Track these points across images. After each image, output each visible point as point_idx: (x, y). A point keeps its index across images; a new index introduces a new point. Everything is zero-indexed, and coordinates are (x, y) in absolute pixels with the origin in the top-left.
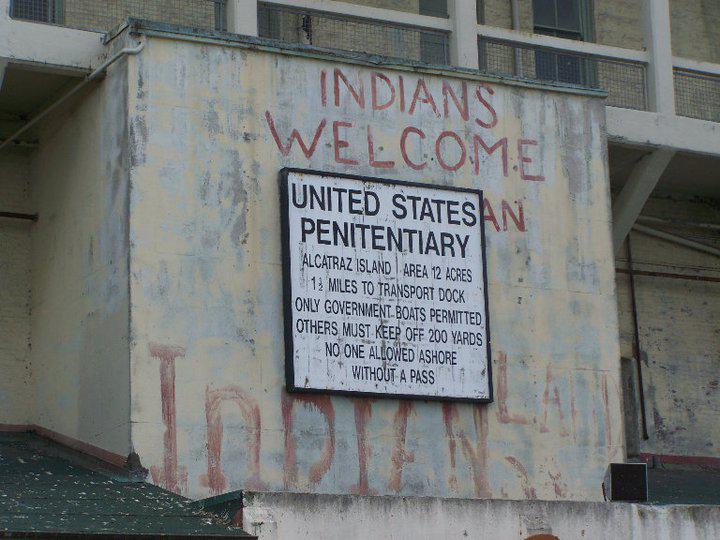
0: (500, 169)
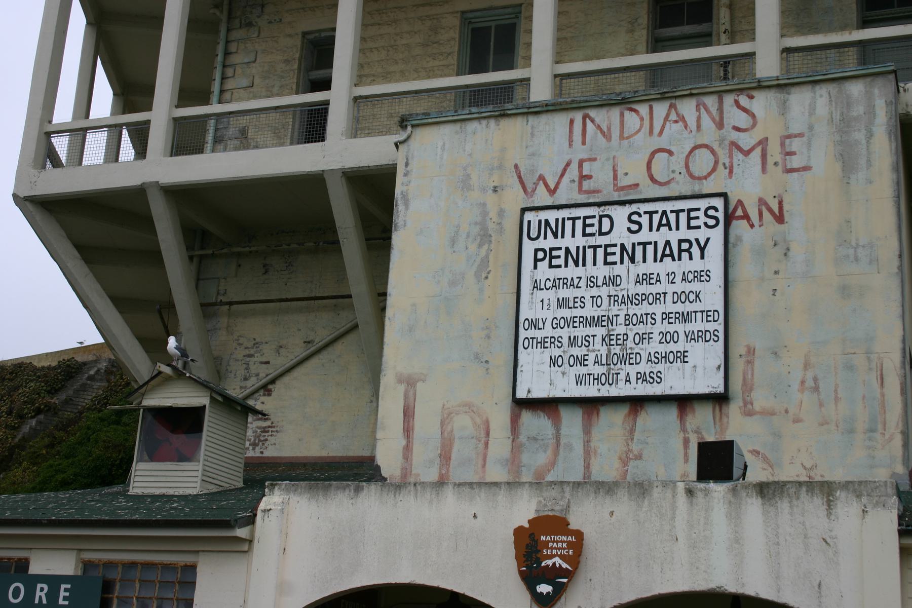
0: (759, 167)
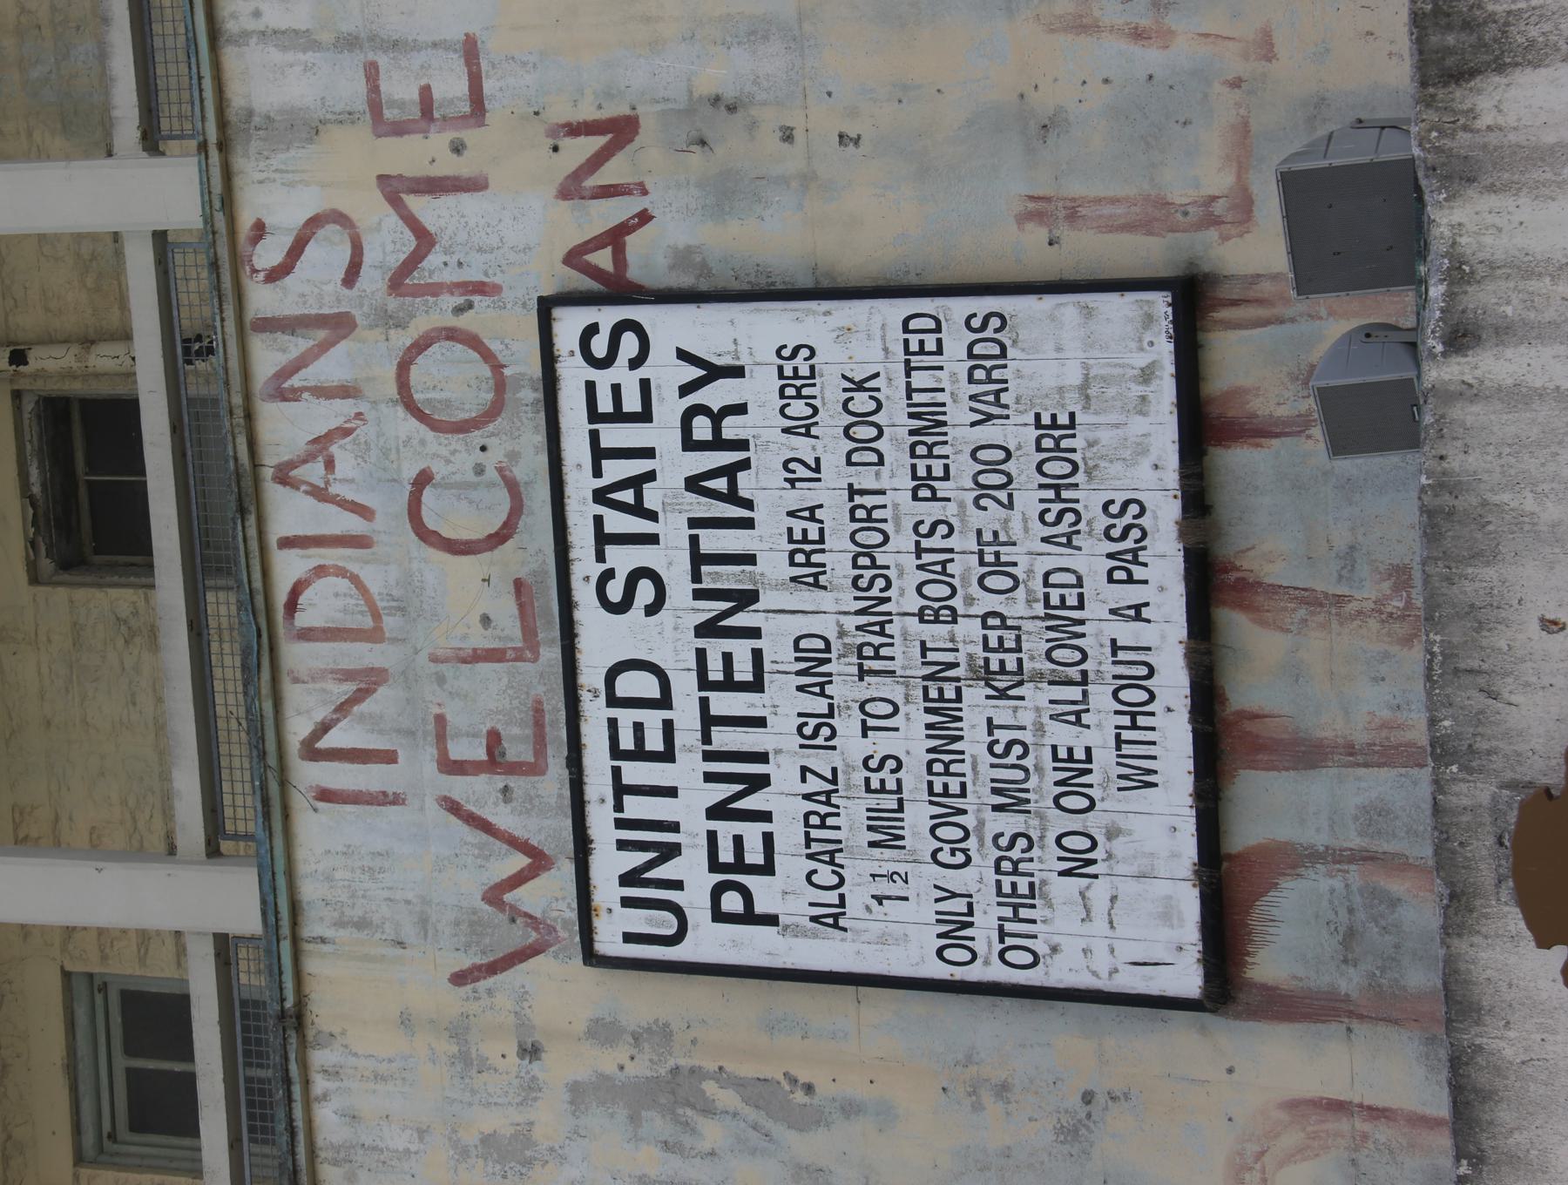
0: (465, 197)
